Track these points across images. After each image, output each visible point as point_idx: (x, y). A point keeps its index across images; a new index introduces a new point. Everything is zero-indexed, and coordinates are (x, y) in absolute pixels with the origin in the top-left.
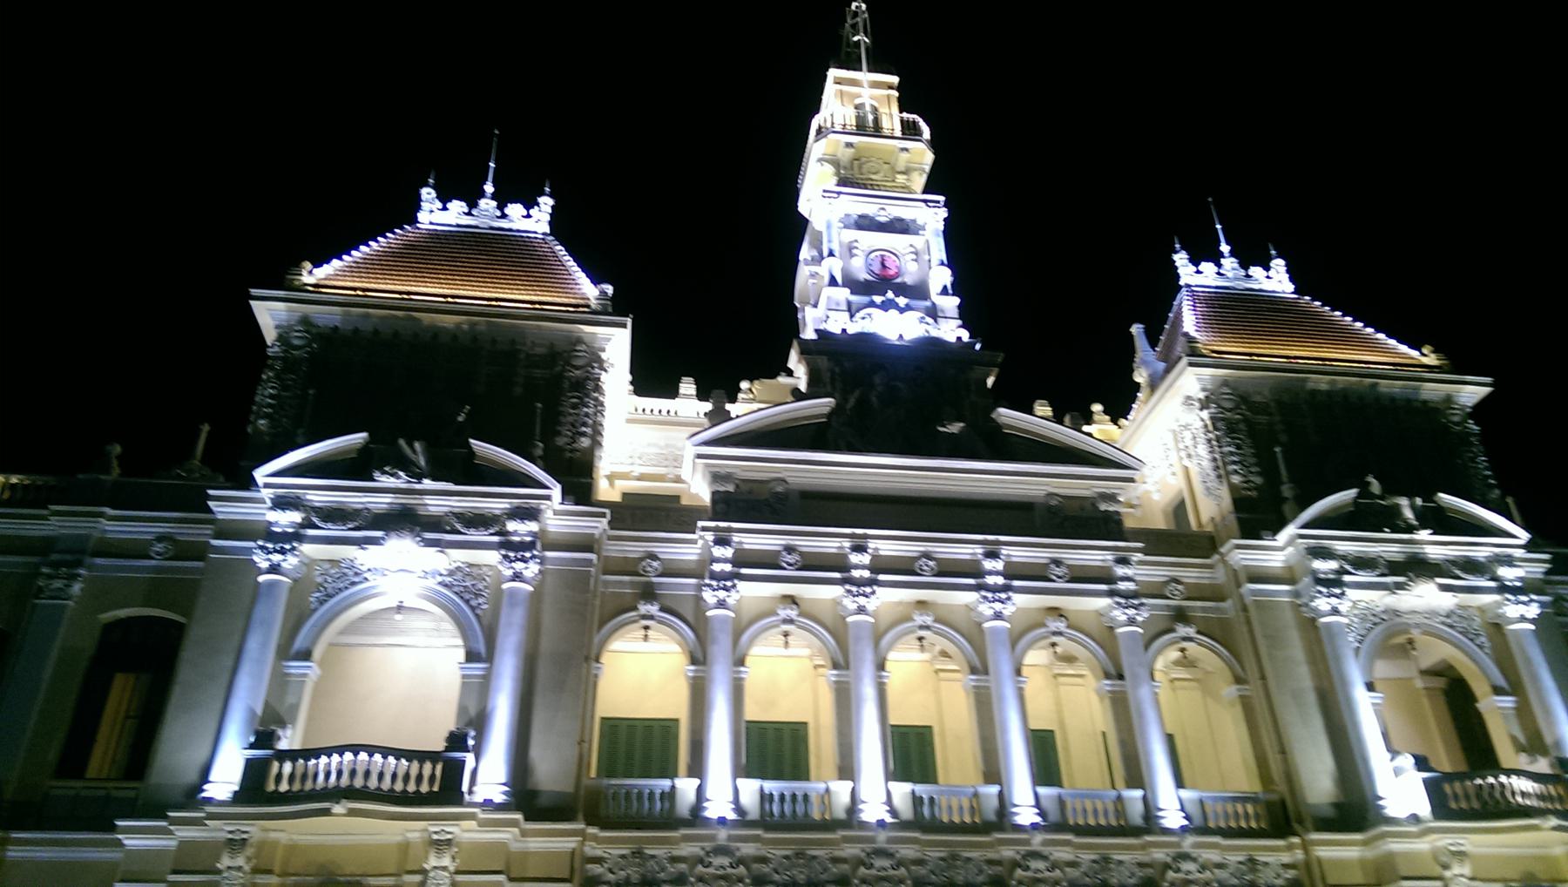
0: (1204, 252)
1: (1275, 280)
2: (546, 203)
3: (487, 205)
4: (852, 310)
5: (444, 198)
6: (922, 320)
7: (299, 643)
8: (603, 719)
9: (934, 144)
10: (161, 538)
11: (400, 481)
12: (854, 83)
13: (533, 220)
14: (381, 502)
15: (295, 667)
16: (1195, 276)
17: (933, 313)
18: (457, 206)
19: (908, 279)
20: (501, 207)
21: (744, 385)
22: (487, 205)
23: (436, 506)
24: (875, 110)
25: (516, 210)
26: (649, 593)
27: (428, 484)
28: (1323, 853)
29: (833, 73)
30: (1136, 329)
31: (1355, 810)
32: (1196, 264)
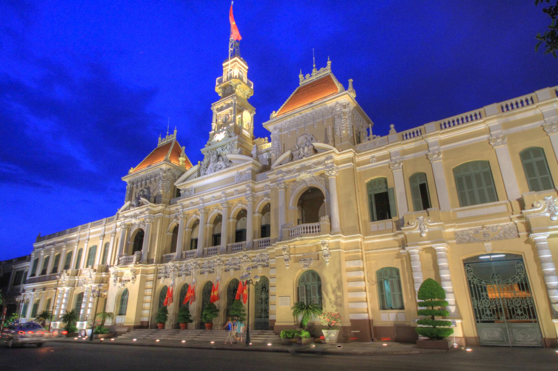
12: (228, 65)
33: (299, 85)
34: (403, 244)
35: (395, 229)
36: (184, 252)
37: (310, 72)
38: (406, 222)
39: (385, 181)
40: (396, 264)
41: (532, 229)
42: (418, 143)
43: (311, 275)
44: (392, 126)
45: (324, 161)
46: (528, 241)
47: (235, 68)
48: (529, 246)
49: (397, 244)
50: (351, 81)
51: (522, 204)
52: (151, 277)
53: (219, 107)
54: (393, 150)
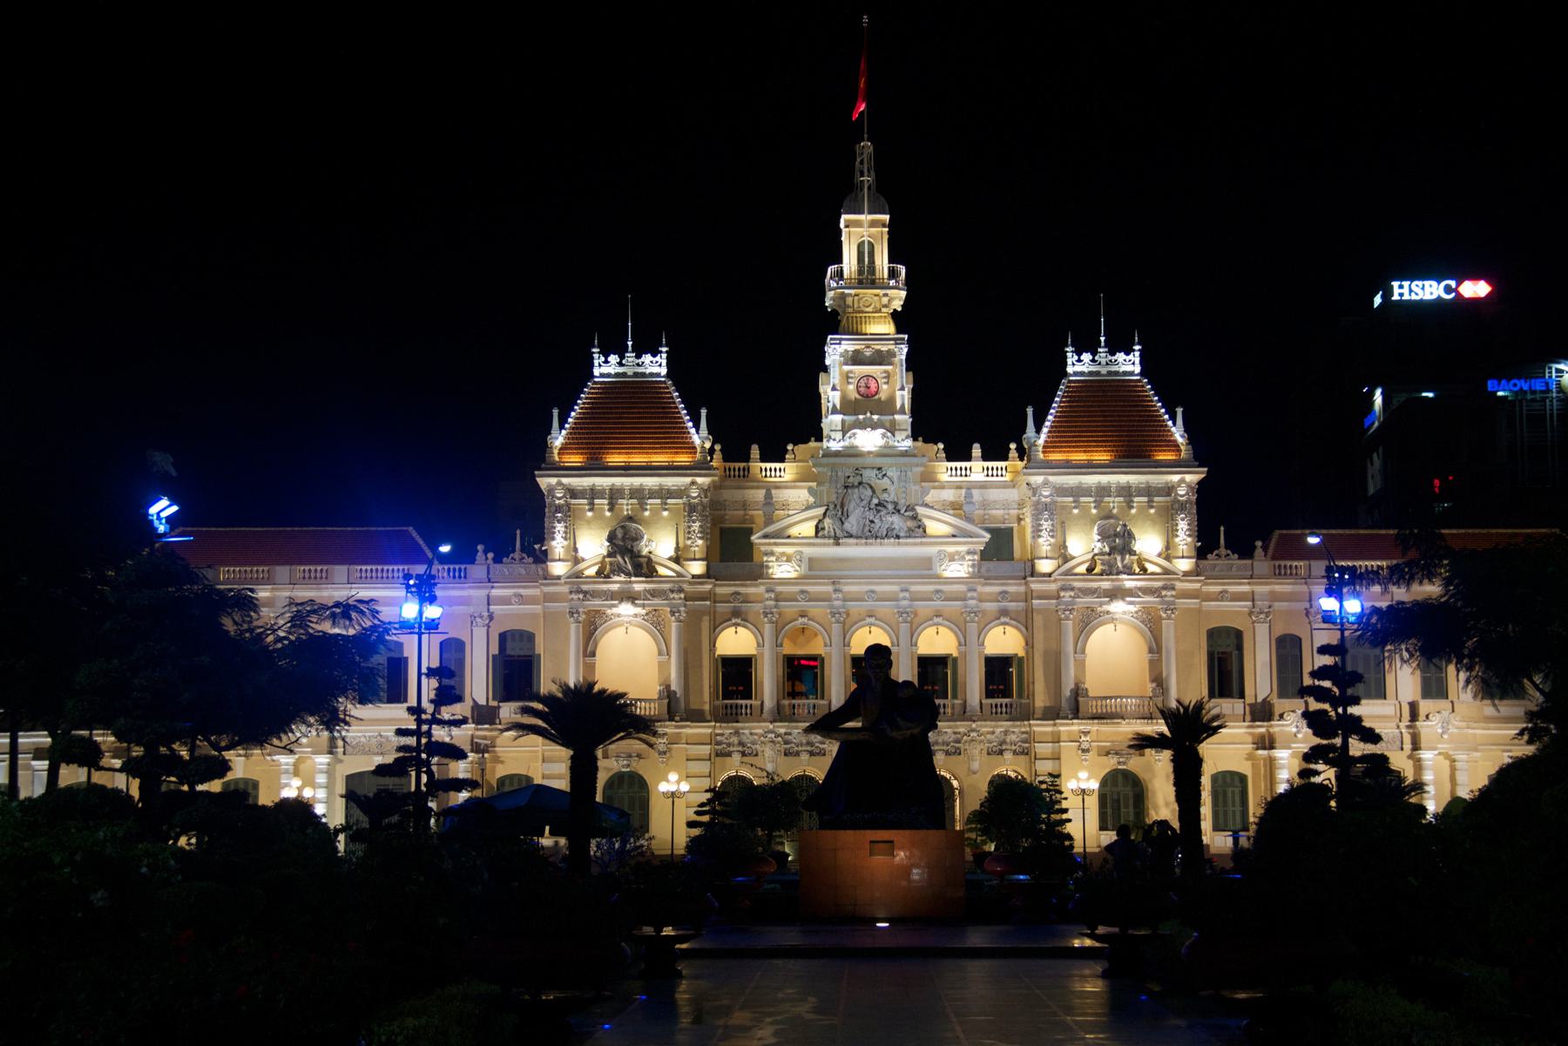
0: (1086, 345)
1: (1129, 364)
3: (630, 357)
4: (844, 431)
6: (884, 436)
9: (910, 284)
11: (622, 578)
12: (858, 224)
13: (655, 365)
14: (615, 587)
16: (1078, 365)
17: (892, 429)
18: (613, 359)
19: (883, 396)
21: (790, 447)
22: (630, 356)
23: (638, 587)
24: (871, 246)
25: (647, 358)
26: (736, 613)
29: (844, 218)
30: (1030, 411)
32: (1079, 355)
33: (1065, 374)
34: (1267, 743)
35: (1248, 717)
36: (786, 702)
37: (1094, 353)
38: (1277, 712)
39: (1239, 635)
40: (1245, 768)
41: (1423, 745)
42: (1298, 588)
43: (1120, 778)
46: (1410, 757)
47: (862, 233)
48: (1411, 762)
49: (1250, 739)
50: (1179, 410)
51: (1413, 707)
52: (706, 750)
53: (851, 348)
54: (1261, 589)
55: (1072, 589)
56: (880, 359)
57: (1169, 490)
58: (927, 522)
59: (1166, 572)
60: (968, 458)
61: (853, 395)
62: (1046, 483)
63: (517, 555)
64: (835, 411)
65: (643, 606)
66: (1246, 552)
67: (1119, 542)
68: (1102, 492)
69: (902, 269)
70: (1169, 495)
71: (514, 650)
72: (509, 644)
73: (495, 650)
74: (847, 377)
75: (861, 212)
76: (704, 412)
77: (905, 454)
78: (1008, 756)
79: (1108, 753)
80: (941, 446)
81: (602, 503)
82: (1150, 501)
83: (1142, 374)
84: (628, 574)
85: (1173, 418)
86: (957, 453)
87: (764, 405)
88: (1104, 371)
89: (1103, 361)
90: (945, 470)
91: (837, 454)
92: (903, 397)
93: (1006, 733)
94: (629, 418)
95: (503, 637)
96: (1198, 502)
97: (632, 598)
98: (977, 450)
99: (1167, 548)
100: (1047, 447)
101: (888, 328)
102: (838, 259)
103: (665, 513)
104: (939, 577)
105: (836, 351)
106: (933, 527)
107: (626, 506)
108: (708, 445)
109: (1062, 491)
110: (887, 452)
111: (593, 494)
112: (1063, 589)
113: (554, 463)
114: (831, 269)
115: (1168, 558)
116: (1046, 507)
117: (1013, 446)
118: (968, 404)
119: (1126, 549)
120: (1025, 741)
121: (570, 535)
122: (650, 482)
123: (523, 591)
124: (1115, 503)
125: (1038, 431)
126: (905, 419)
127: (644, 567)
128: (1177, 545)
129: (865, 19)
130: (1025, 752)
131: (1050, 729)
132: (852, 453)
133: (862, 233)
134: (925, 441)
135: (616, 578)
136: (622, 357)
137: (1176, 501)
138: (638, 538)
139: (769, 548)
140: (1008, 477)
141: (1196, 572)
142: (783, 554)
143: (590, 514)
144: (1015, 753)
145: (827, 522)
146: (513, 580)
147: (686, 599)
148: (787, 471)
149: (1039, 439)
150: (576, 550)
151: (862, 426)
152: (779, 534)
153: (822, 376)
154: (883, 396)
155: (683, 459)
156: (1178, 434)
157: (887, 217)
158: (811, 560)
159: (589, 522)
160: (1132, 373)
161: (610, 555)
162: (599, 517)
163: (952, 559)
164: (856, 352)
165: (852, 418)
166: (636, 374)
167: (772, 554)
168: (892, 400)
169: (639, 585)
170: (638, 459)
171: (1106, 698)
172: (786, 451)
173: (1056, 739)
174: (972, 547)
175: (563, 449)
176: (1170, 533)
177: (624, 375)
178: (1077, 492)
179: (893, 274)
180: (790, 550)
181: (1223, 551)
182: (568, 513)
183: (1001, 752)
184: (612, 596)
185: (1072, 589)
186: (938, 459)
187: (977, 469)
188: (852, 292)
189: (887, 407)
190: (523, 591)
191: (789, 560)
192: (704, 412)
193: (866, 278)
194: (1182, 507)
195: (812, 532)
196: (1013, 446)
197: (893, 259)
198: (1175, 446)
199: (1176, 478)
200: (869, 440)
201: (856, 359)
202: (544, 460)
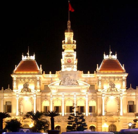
0: (108, 54)
1: (115, 57)
2: (34, 55)
3: (29, 56)
5: (24, 56)
7: (20, 104)
8: (44, 107)
9: (77, 43)
10: (8, 95)
12: (68, 34)
13: (33, 58)
14: (24, 94)
15: (20, 106)
16: (106, 57)
20: (30, 56)
22: (29, 56)
25: (31, 57)
27: (27, 92)
28: (98, 118)
29: (65, 33)
30: (98, 65)
31: (101, 115)
33: (104, 59)
35: (135, 116)
37: (109, 55)
39: (133, 102)
44: (137, 87)
45: (120, 94)
47: (69, 36)
55: (104, 94)
56: (71, 56)
57: (121, 77)
58: (79, 83)
59: (121, 91)
60: (87, 73)
61: (66, 62)
62: (100, 76)
63: (9, 89)
64: (63, 64)
65: (29, 97)
66: (135, 88)
67: (113, 86)
68: (110, 78)
69: (75, 41)
70: (121, 78)
71: (8, 104)
72: (7, 103)
73: (5, 104)
74: (65, 59)
75: (68, 32)
76: (41, 65)
77: (75, 72)
78: (93, 122)
79: (110, 122)
80: (82, 71)
81: (23, 80)
82: (118, 79)
83: (117, 59)
84: (26, 91)
85: (122, 66)
86: (85, 72)
87: (51, 64)
88: (110, 58)
89: (110, 57)
90: (84, 76)
91: (63, 72)
92: (76, 62)
93: (92, 118)
94: (28, 66)
95: (6, 102)
96: (126, 79)
97: (27, 95)
98: (89, 72)
99: (121, 87)
100: (100, 70)
101: (73, 51)
102: (64, 39)
103: (33, 81)
104: (81, 92)
105: (64, 54)
106: (80, 84)
107: (27, 80)
108: (41, 71)
109: (102, 77)
110: (72, 71)
111: (21, 78)
112: (103, 94)
113: (14, 73)
114: (63, 41)
115: (121, 89)
116: (100, 80)
117: (95, 71)
118: (87, 63)
119: (114, 87)
120: (96, 120)
121: (17, 85)
122: (31, 76)
123: (10, 95)
124: (112, 80)
125: (99, 67)
126: (75, 67)
127: (29, 91)
128: (123, 87)
129: (69, 1)
130: (96, 122)
131: (100, 118)
132: (66, 71)
133: (69, 36)
134: (80, 71)
135: (24, 92)
136: (27, 57)
137: (123, 79)
138: (28, 85)
139: (51, 87)
140: (94, 77)
141: (126, 91)
142: (54, 88)
143: (20, 82)
144: (94, 122)
145: (61, 83)
146: (7, 92)
147: (36, 96)
148: (56, 75)
149: (98, 69)
150: (17, 87)
151: (68, 67)
152: (53, 85)
153: (61, 59)
154: (72, 62)
155: (36, 72)
156: (123, 68)
157: (73, 33)
158: (59, 89)
159: (20, 83)
160: (115, 59)
161: (23, 88)
162: (22, 82)
163: (83, 89)
164: (67, 55)
165: (66, 66)
166: (29, 59)
167: (52, 88)
168: (73, 63)
169: (28, 93)
170: (29, 72)
171: (109, 112)
172: (56, 72)
173: (101, 119)
174: (87, 87)
175: (16, 71)
176: (122, 84)
177: (27, 59)
178: (105, 78)
179: (74, 42)
180: (55, 88)
181: (131, 88)
182: (17, 81)
183: (91, 122)
184: (24, 95)
185: (104, 94)
186: (82, 74)
187: (89, 75)
188: (67, 45)
189: (73, 64)
190: (10, 95)
191: (55, 89)
192: (41, 65)
193: (69, 43)
194: (124, 80)
195: (59, 85)
196: (95, 71)
197: (73, 40)
198: (123, 70)
199: (122, 75)
200: (69, 69)
201: (67, 56)
202: (12, 73)
